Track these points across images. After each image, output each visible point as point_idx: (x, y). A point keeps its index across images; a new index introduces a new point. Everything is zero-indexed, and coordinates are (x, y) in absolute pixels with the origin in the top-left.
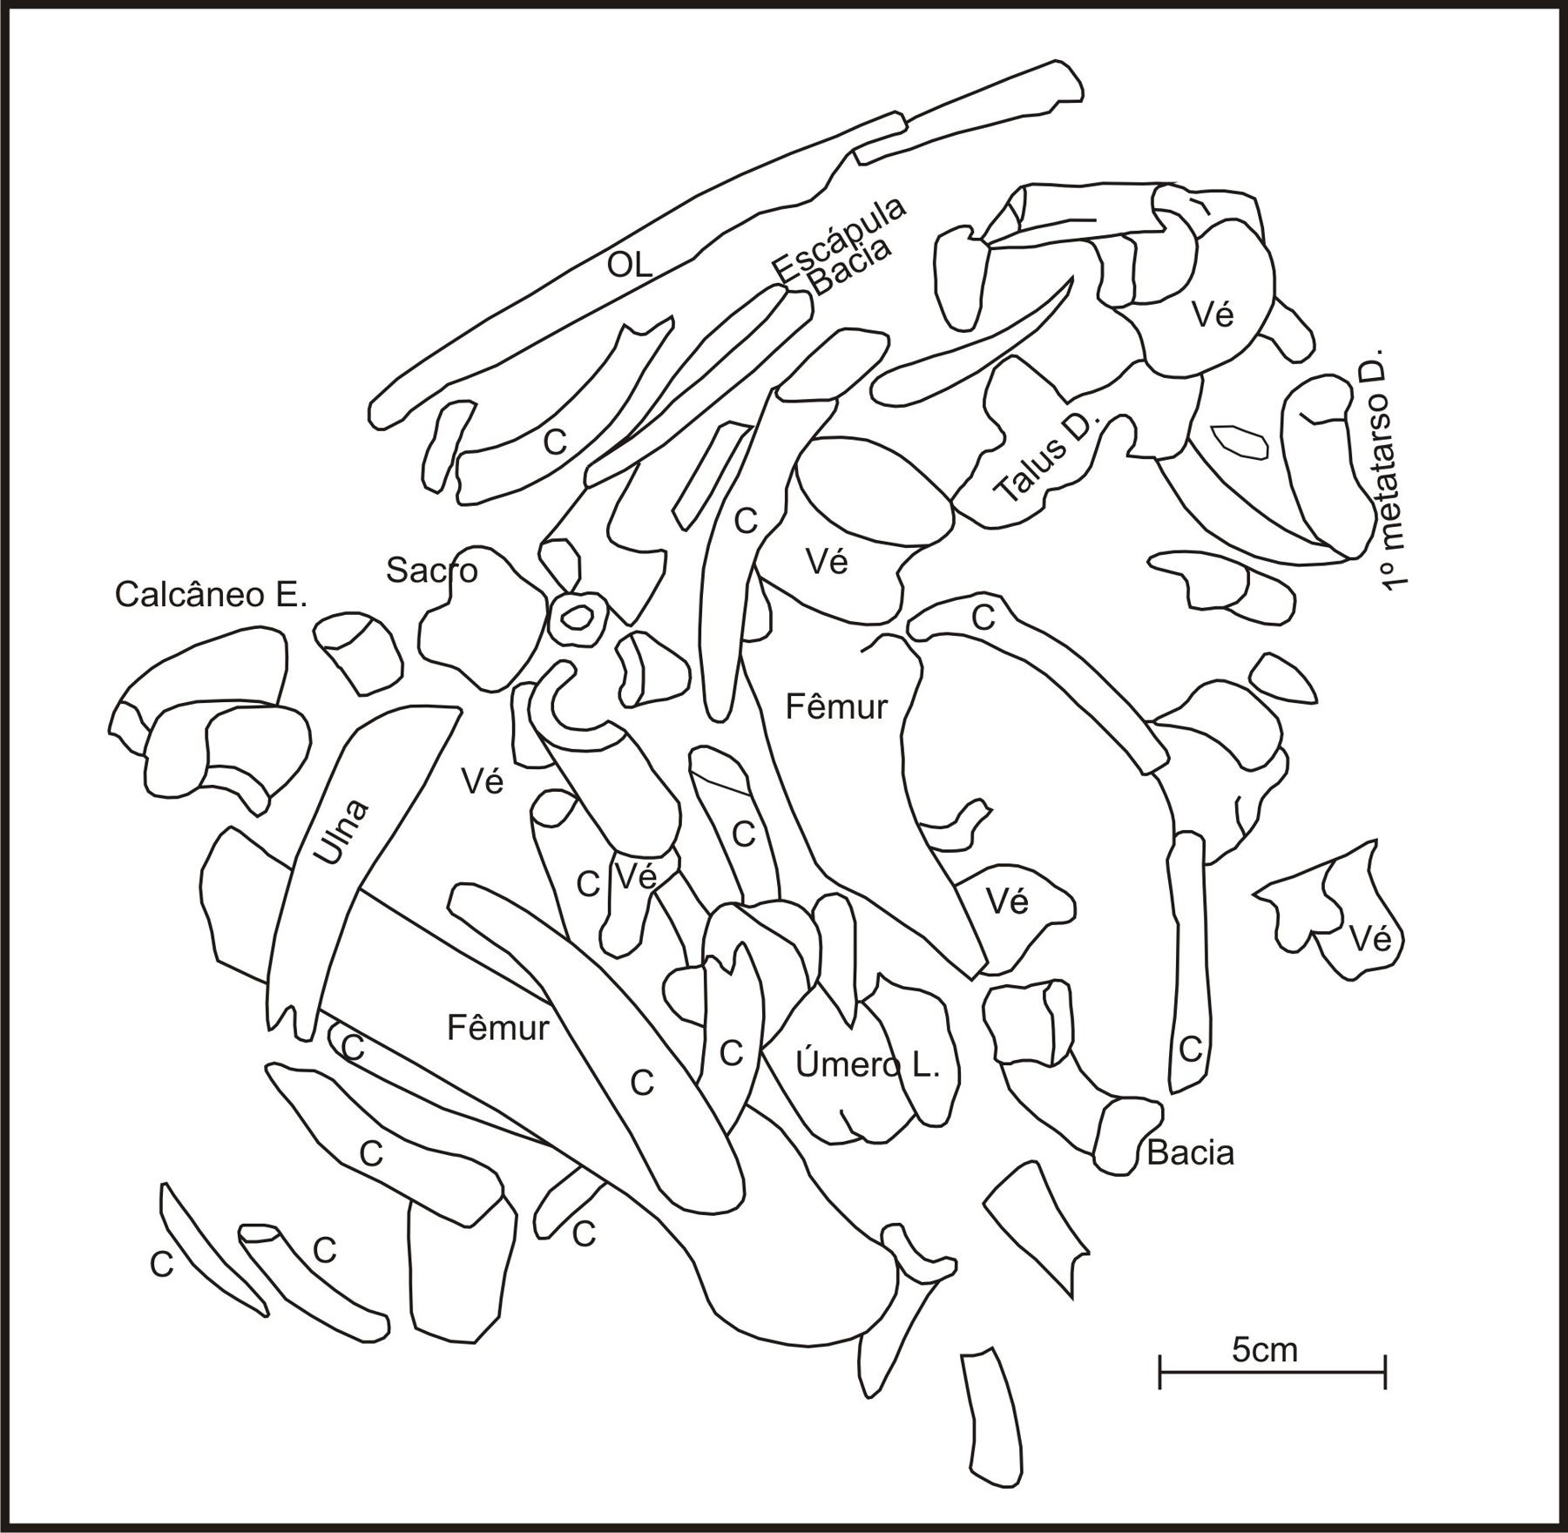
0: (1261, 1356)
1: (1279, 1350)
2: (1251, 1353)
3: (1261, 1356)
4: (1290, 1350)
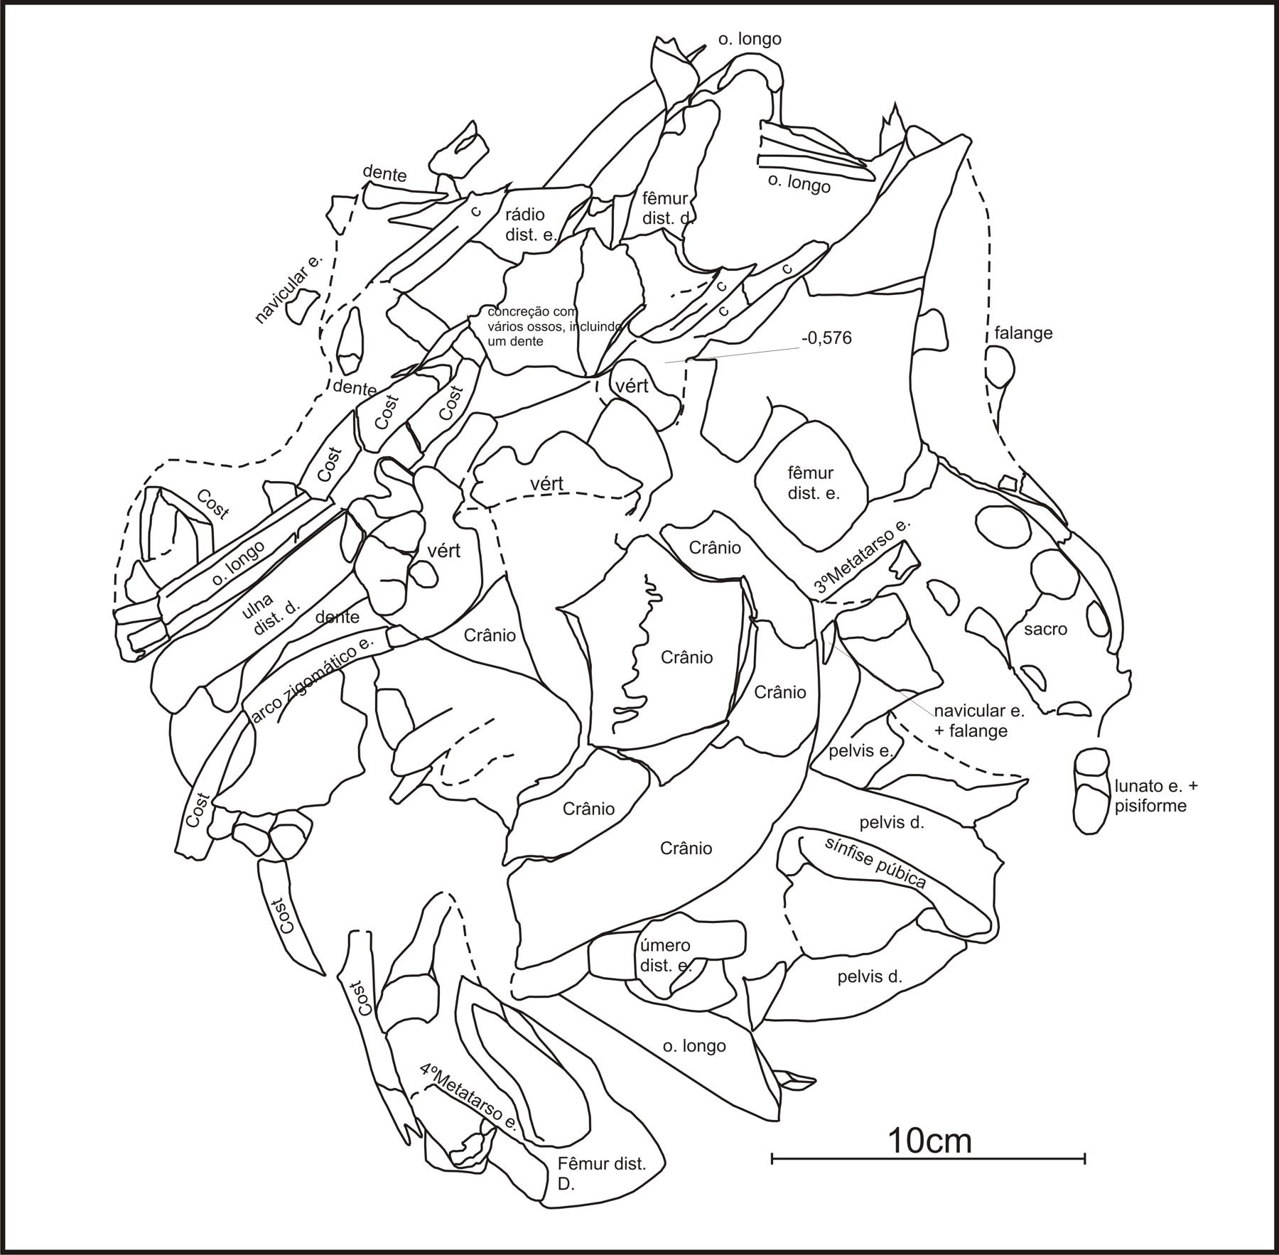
0: (935, 1146)
1: (953, 1141)
2: (926, 1142)
3: (935, 1146)
4: (964, 1141)
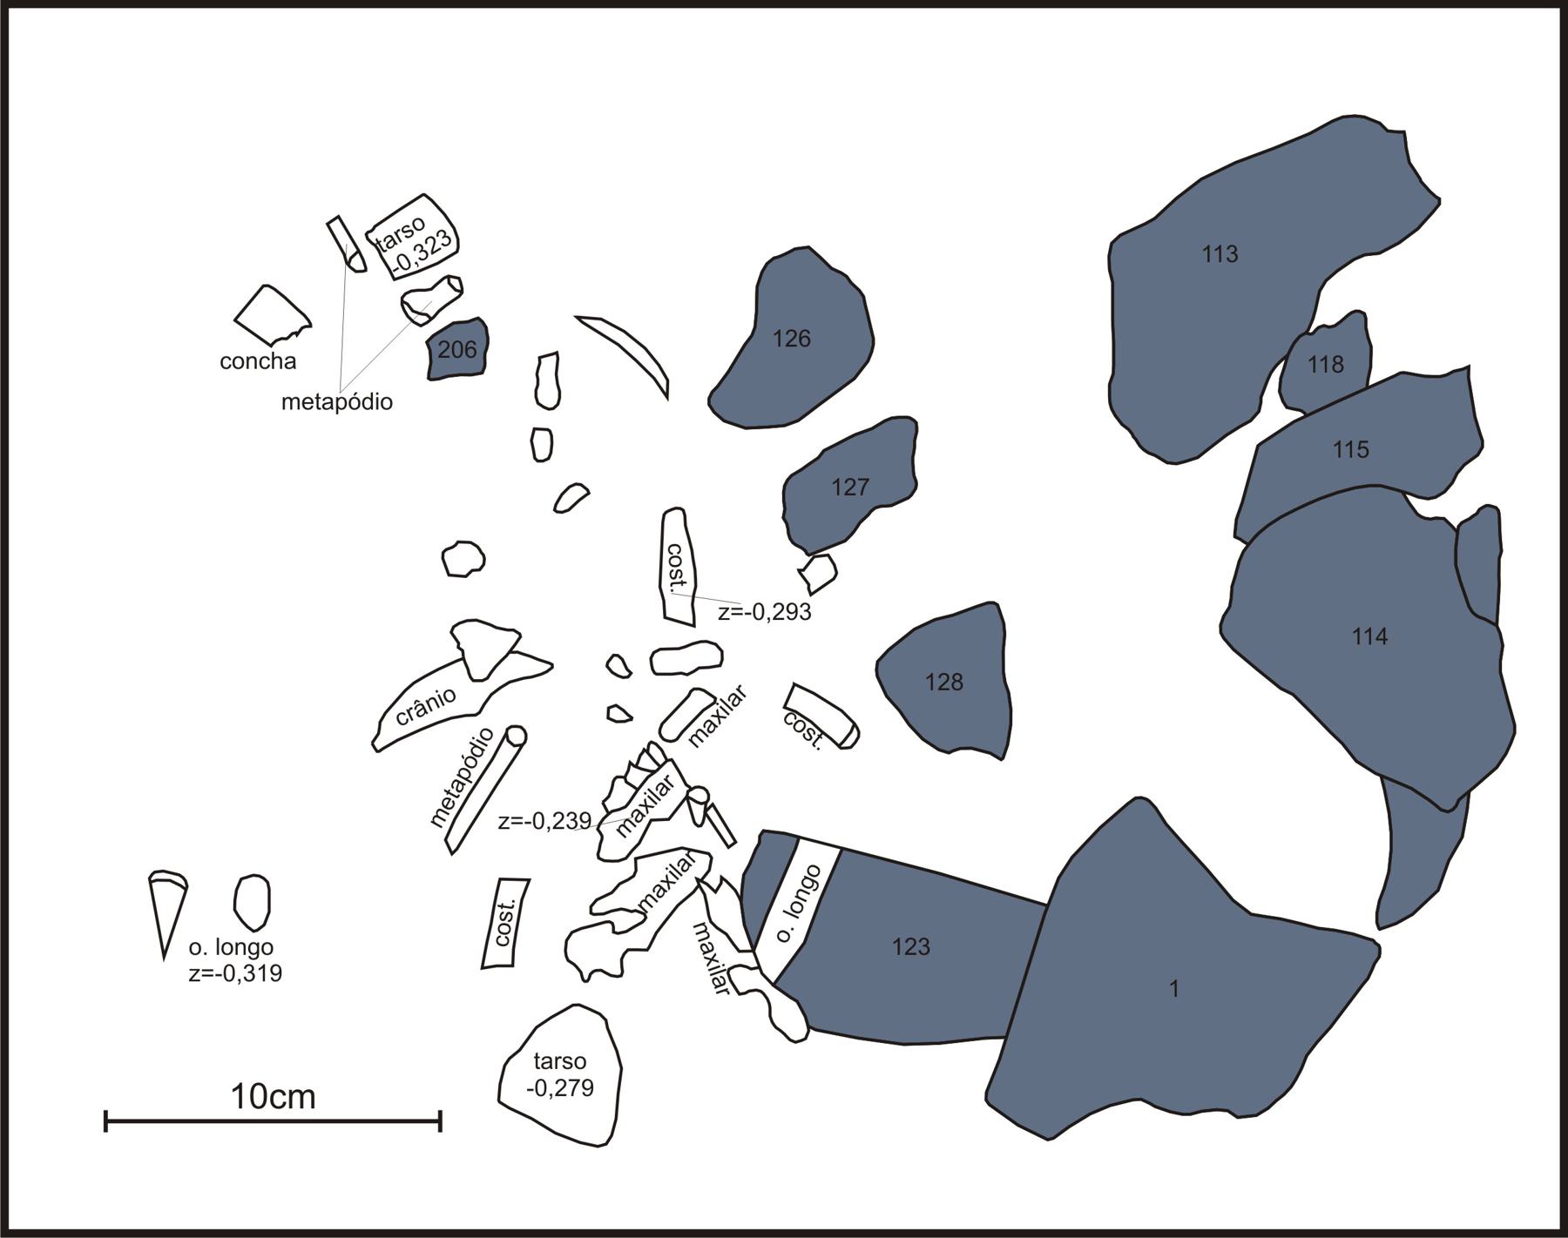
0: (278, 1103)
1: (296, 1096)
2: (269, 1098)
3: (278, 1103)
4: (307, 1096)
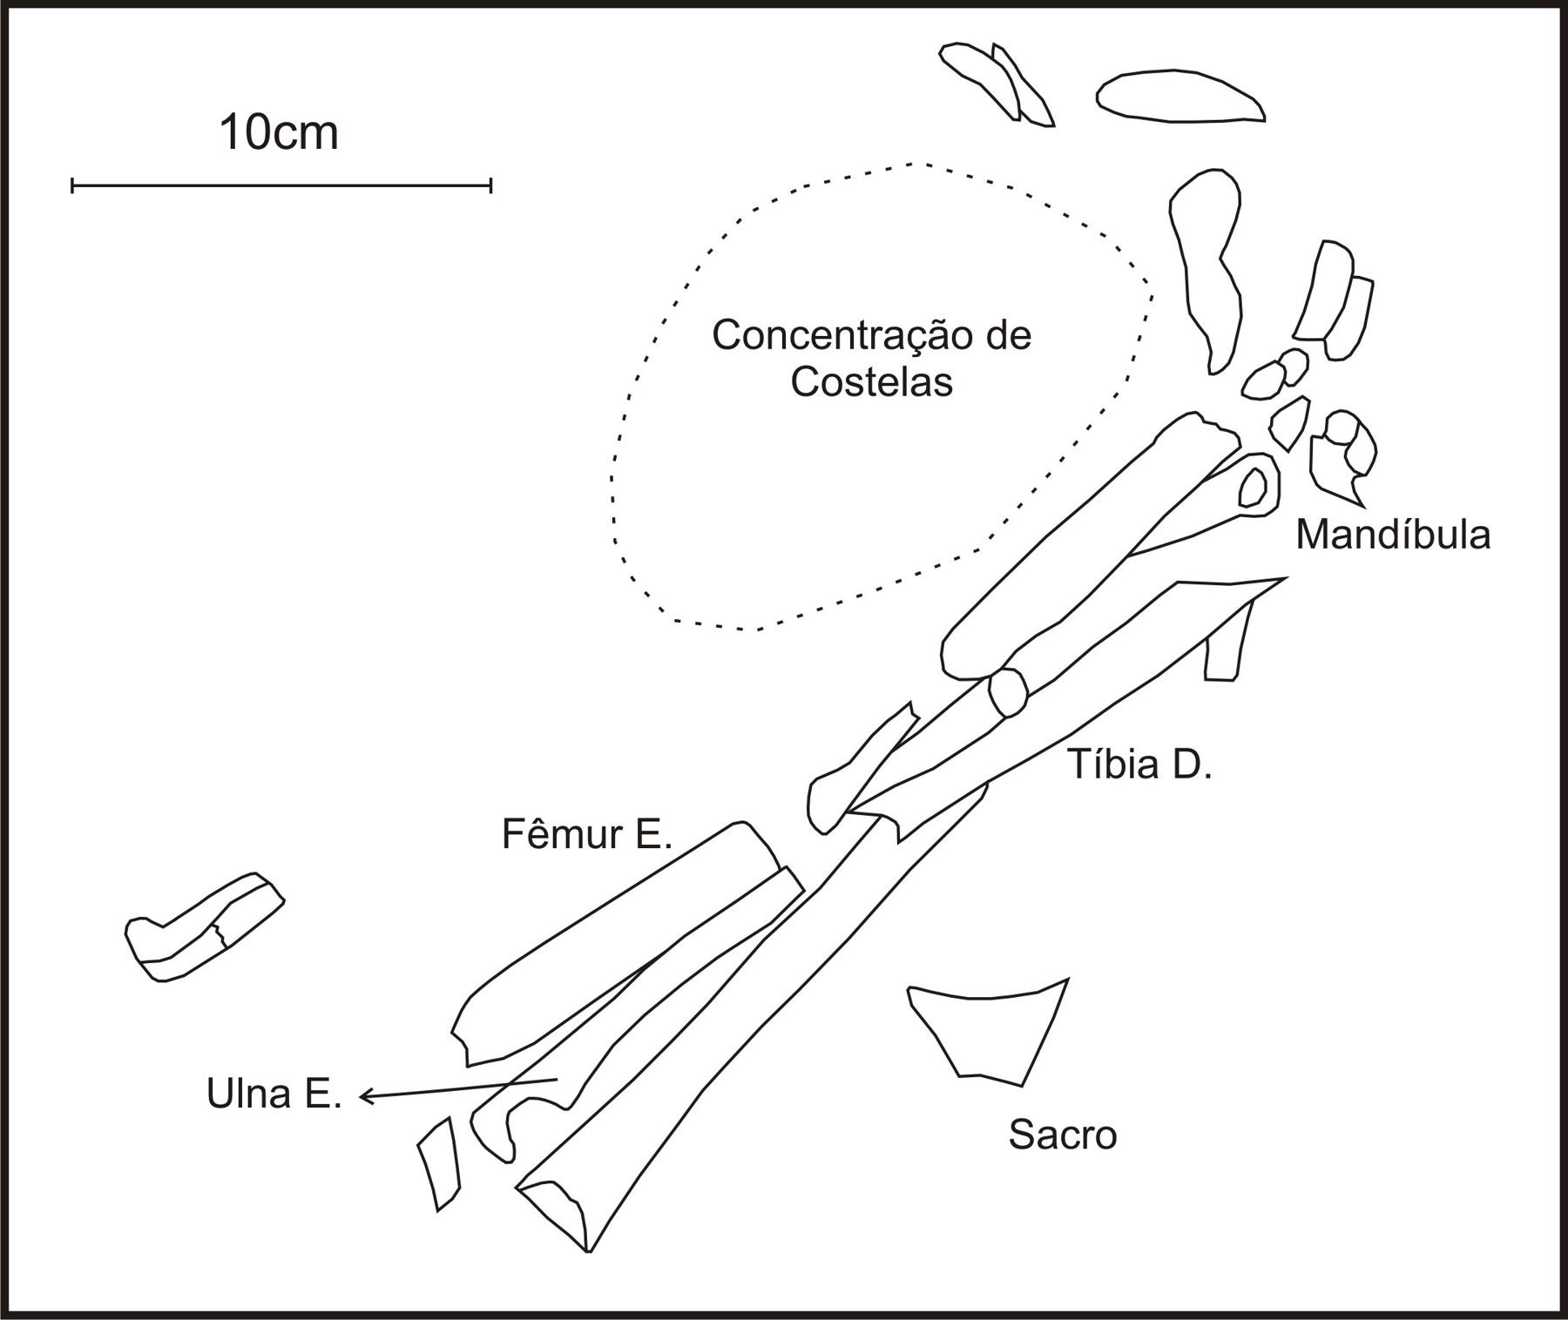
0: (285, 141)
1: (311, 132)
2: (273, 134)
3: (285, 141)
4: (327, 132)
